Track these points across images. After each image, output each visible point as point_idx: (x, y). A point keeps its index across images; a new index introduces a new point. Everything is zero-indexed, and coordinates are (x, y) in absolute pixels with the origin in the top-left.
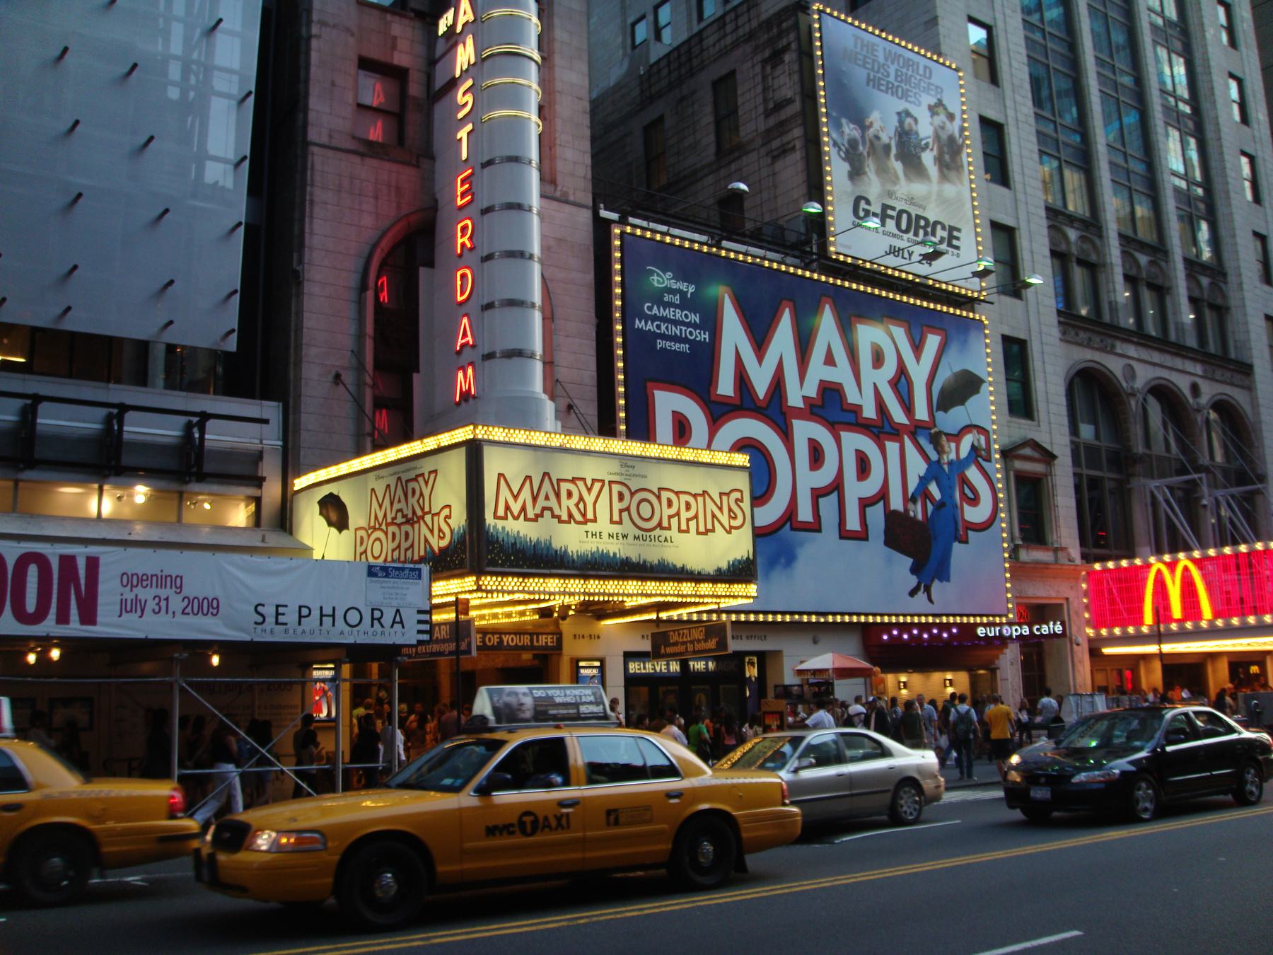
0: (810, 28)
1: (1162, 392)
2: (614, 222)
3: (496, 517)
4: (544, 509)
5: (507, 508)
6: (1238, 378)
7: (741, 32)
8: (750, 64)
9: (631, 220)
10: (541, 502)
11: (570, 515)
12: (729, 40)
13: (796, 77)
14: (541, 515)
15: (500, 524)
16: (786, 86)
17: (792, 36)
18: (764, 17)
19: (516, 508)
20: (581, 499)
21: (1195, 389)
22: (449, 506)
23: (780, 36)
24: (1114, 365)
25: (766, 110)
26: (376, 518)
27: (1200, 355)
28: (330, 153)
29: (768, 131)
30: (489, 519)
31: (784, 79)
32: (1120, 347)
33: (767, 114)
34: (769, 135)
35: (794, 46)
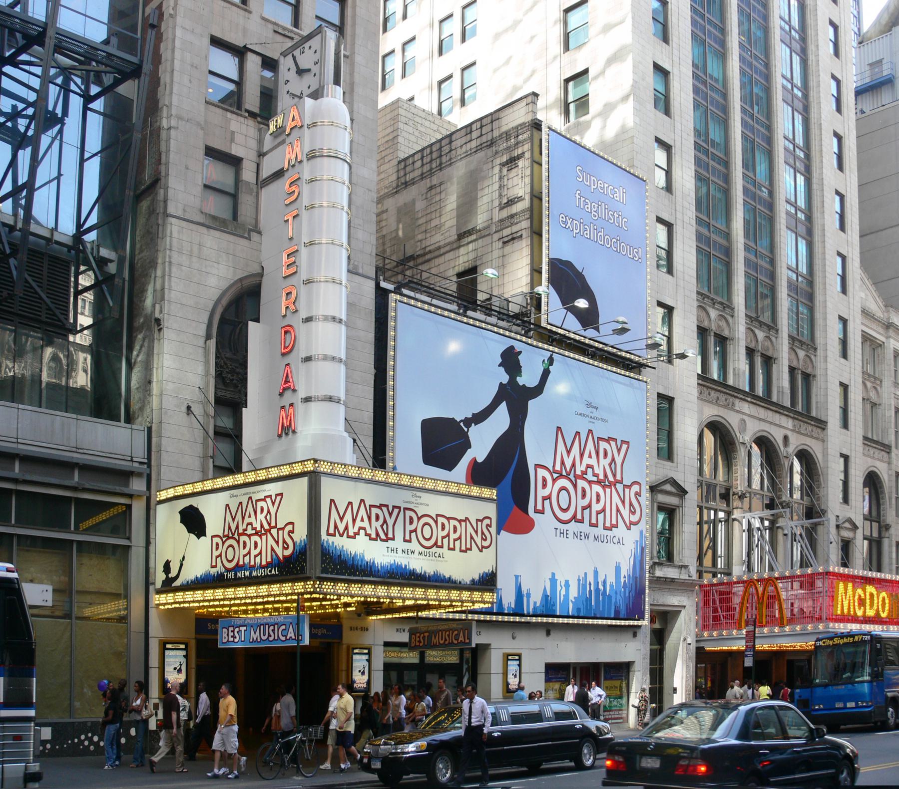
2: (391, 292)
3: (328, 534)
4: (360, 528)
5: (336, 527)
7: (484, 139)
8: (490, 165)
9: (405, 291)
10: (359, 523)
11: (377, 534)
12: (474, 144)
13: (528, 180)
14: (358, 533)
15: (331, 539)
16: (520, 186)
18: (504, 129)
19: (341, 527)
20: (385, 521)
22: (292, 523)
25: (500, 204)
26: (230, 528)
28: (184, 224)
29: (501, 221)
30: (324, 536)
31: (517, 180)
33: (501, 209)
35: (528, 155)
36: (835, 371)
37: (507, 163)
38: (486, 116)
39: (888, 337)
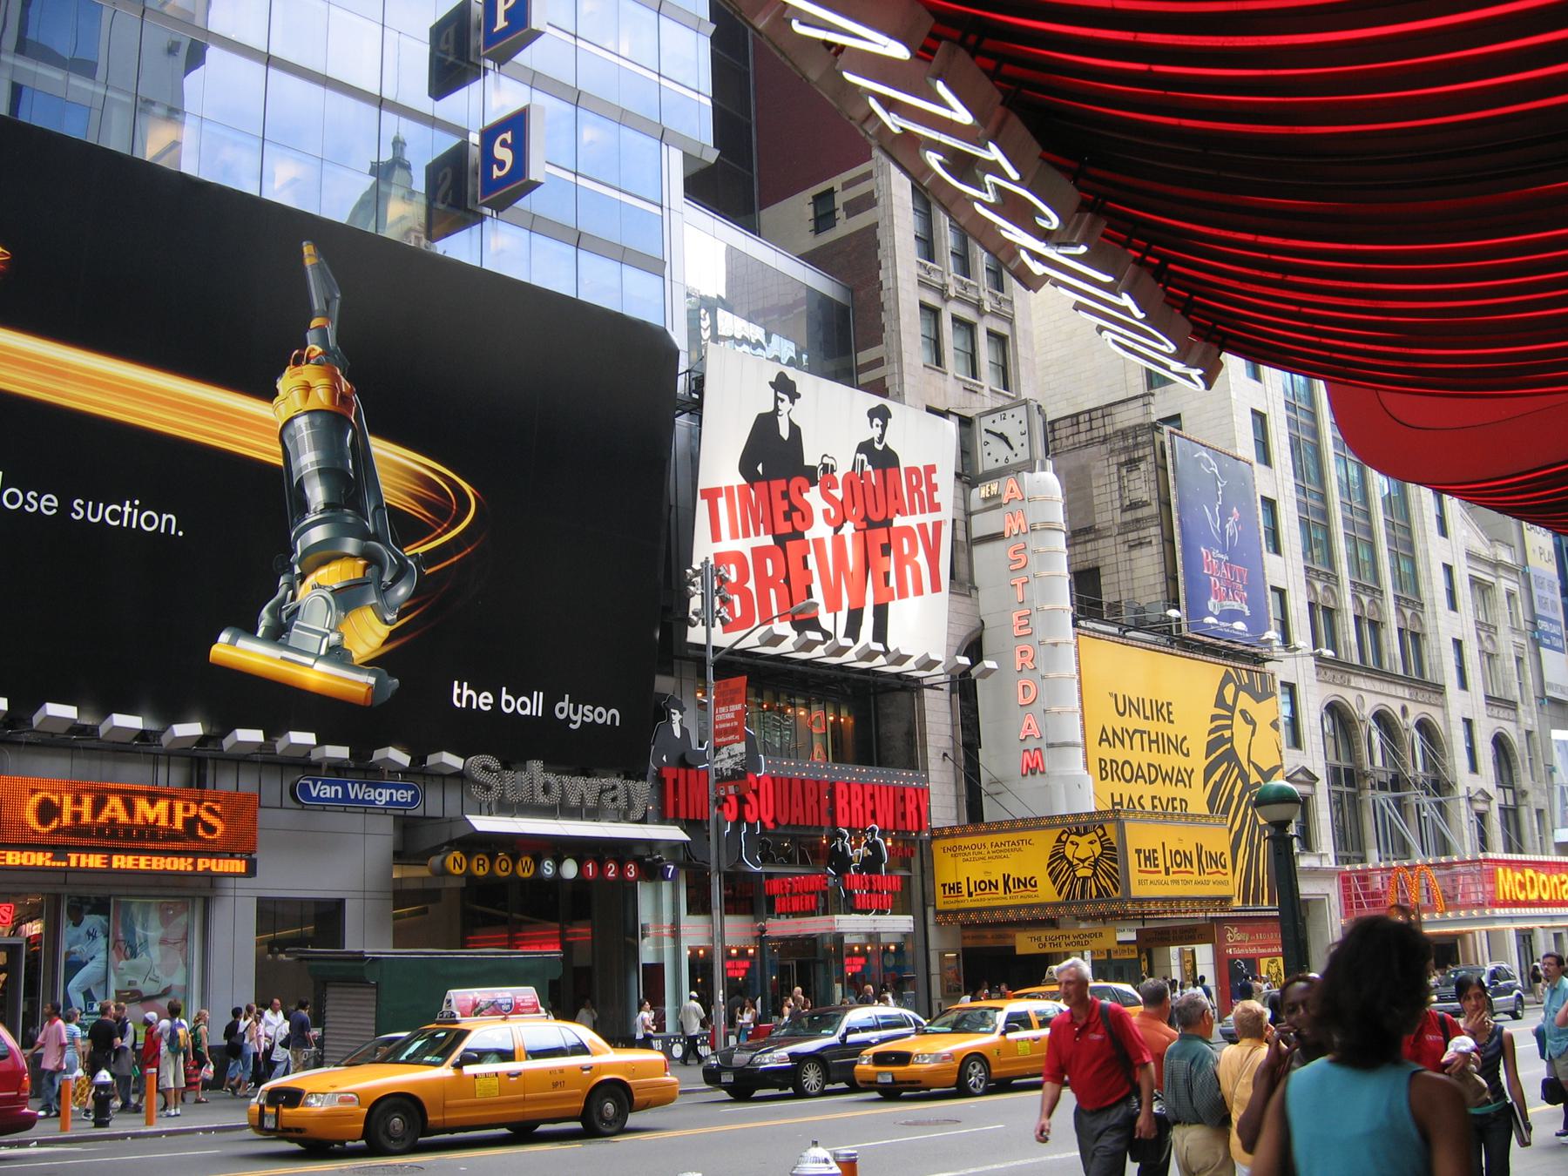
0: (1162, 443)
1: (1382, 718)
6: (1434, 698)
7: (1095, 433)
12: (1083, 437)
13: (1153, 485)
16: (1141, 486)
17: (1148, 450)
18: (1119, 426)
21: (1404, 710)
23: (1136, 446)
24: (1350, 697)
27: (1404, 680)
31: (1138, 484)
32: (1355, 681)
33: (1124, 511)
34: (1125, 528)
35: (1150, 459)
36: (1448, 626)
37: (1126, 463)
38: (1096, 409)
39: (1497, 577)
